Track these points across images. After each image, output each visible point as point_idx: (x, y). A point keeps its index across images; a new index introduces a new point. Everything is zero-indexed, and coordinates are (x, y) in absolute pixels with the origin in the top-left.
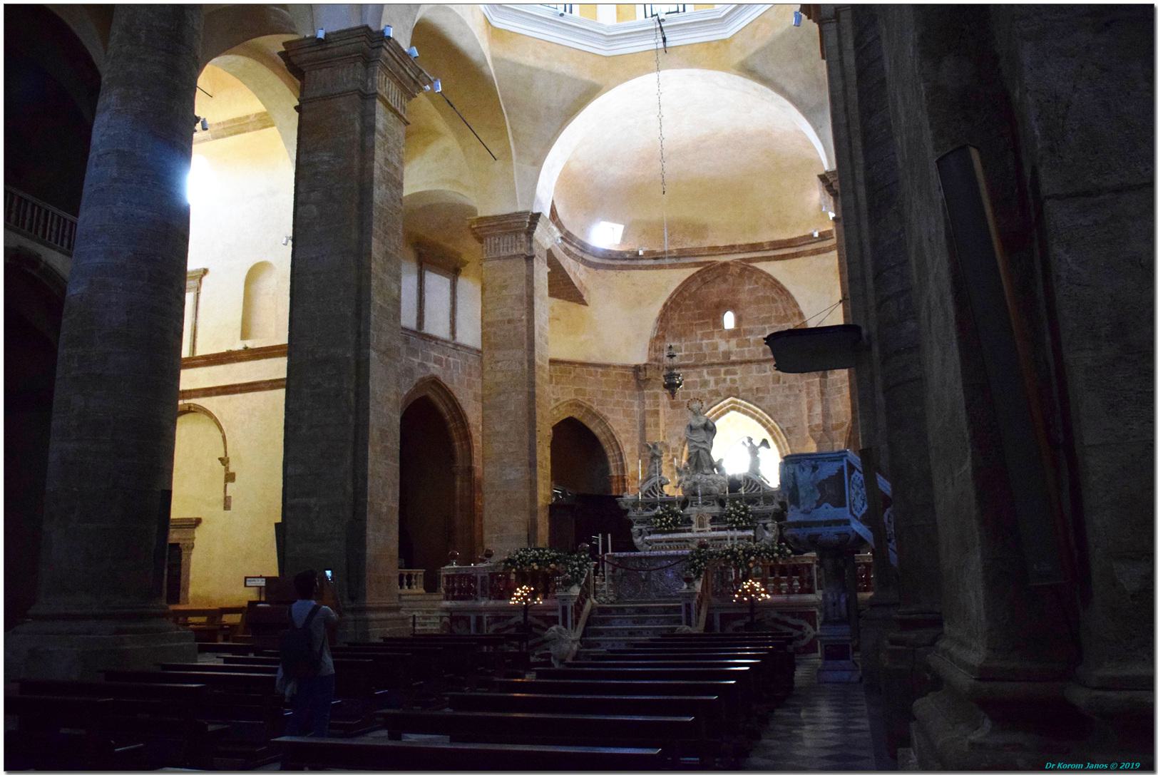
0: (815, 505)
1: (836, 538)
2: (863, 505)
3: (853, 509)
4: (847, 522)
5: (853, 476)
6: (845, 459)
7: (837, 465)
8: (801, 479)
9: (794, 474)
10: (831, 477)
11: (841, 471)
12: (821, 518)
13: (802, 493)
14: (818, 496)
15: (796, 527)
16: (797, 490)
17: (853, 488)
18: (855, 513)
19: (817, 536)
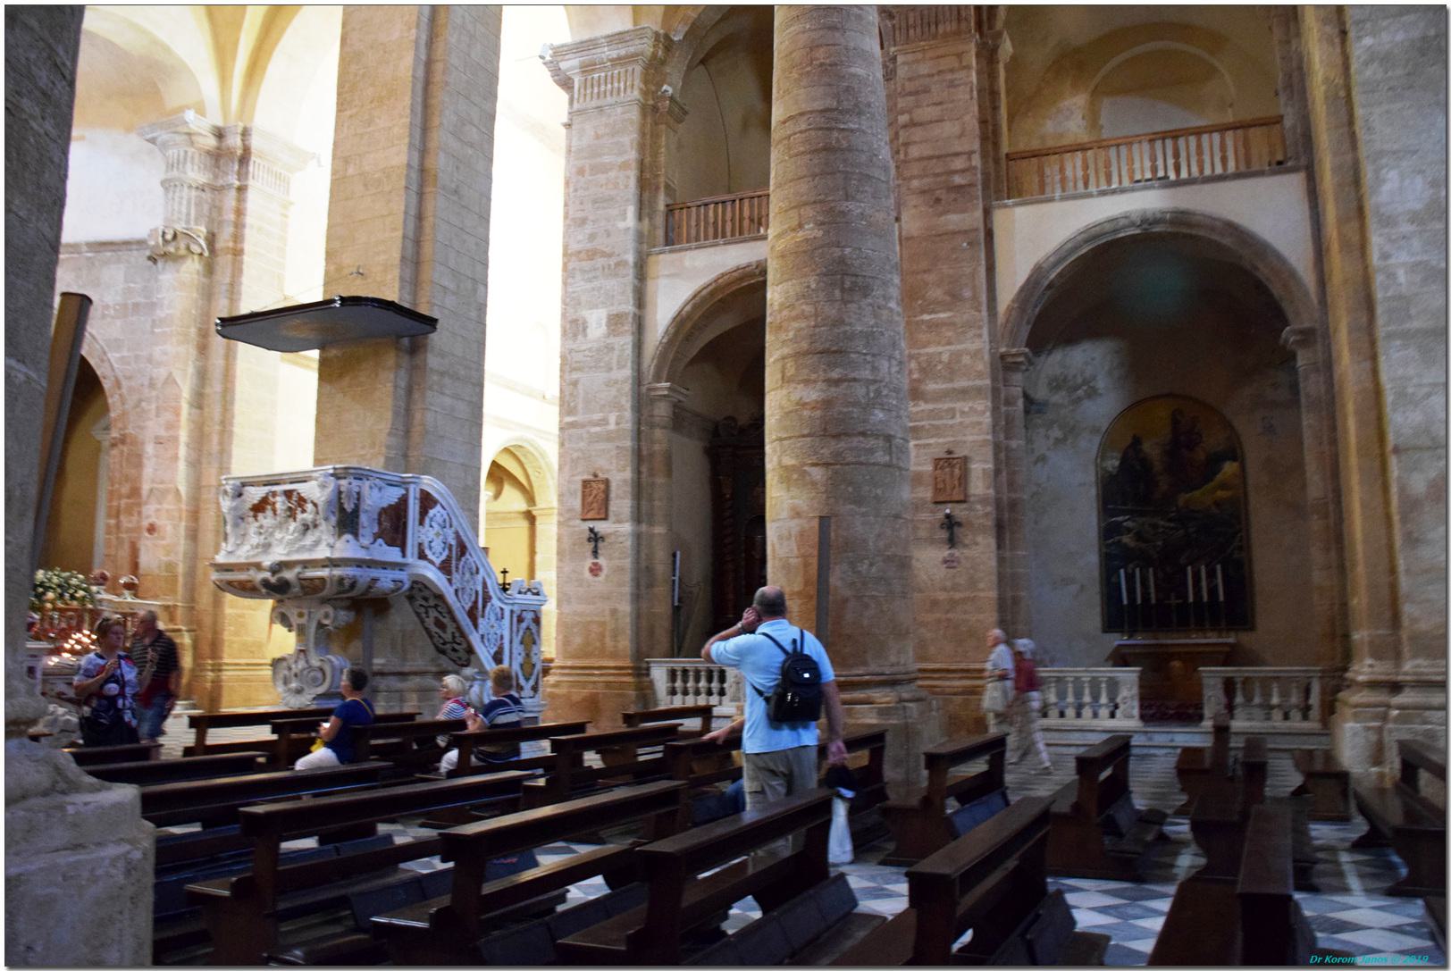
0: (372, 540)
1: (392, 585)
2: (444, 549)
3: (427, 552)
4: (401, 567)
5: (431, 513)
6: (412, 487)
7: (399, 492)
8: (368, 502)
9: (358, 493)
10: (390, 506)
11: (404, 501)
12: (378, 557)
13: (363, 519)
14: (376, 529)
15: (358, 566)
16: (357, 517)
17: (431, 526)
18: (430, 556)
19: (375, 580)
